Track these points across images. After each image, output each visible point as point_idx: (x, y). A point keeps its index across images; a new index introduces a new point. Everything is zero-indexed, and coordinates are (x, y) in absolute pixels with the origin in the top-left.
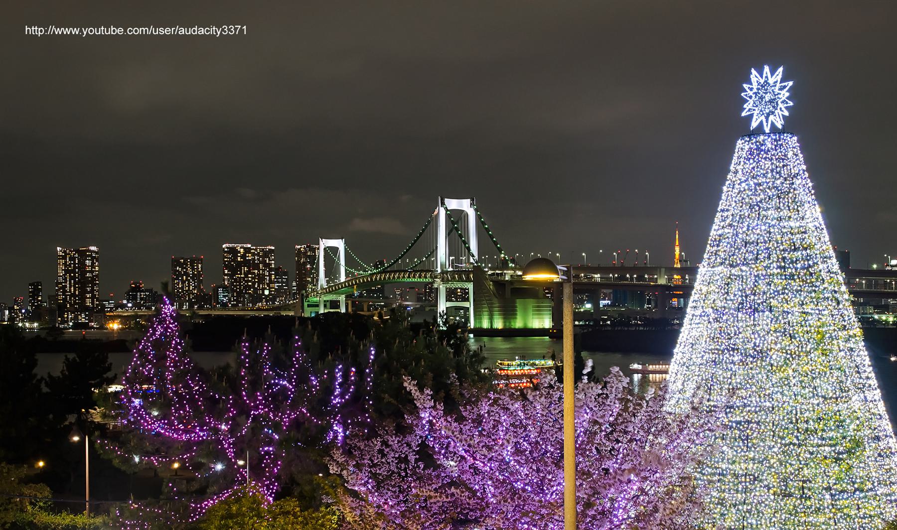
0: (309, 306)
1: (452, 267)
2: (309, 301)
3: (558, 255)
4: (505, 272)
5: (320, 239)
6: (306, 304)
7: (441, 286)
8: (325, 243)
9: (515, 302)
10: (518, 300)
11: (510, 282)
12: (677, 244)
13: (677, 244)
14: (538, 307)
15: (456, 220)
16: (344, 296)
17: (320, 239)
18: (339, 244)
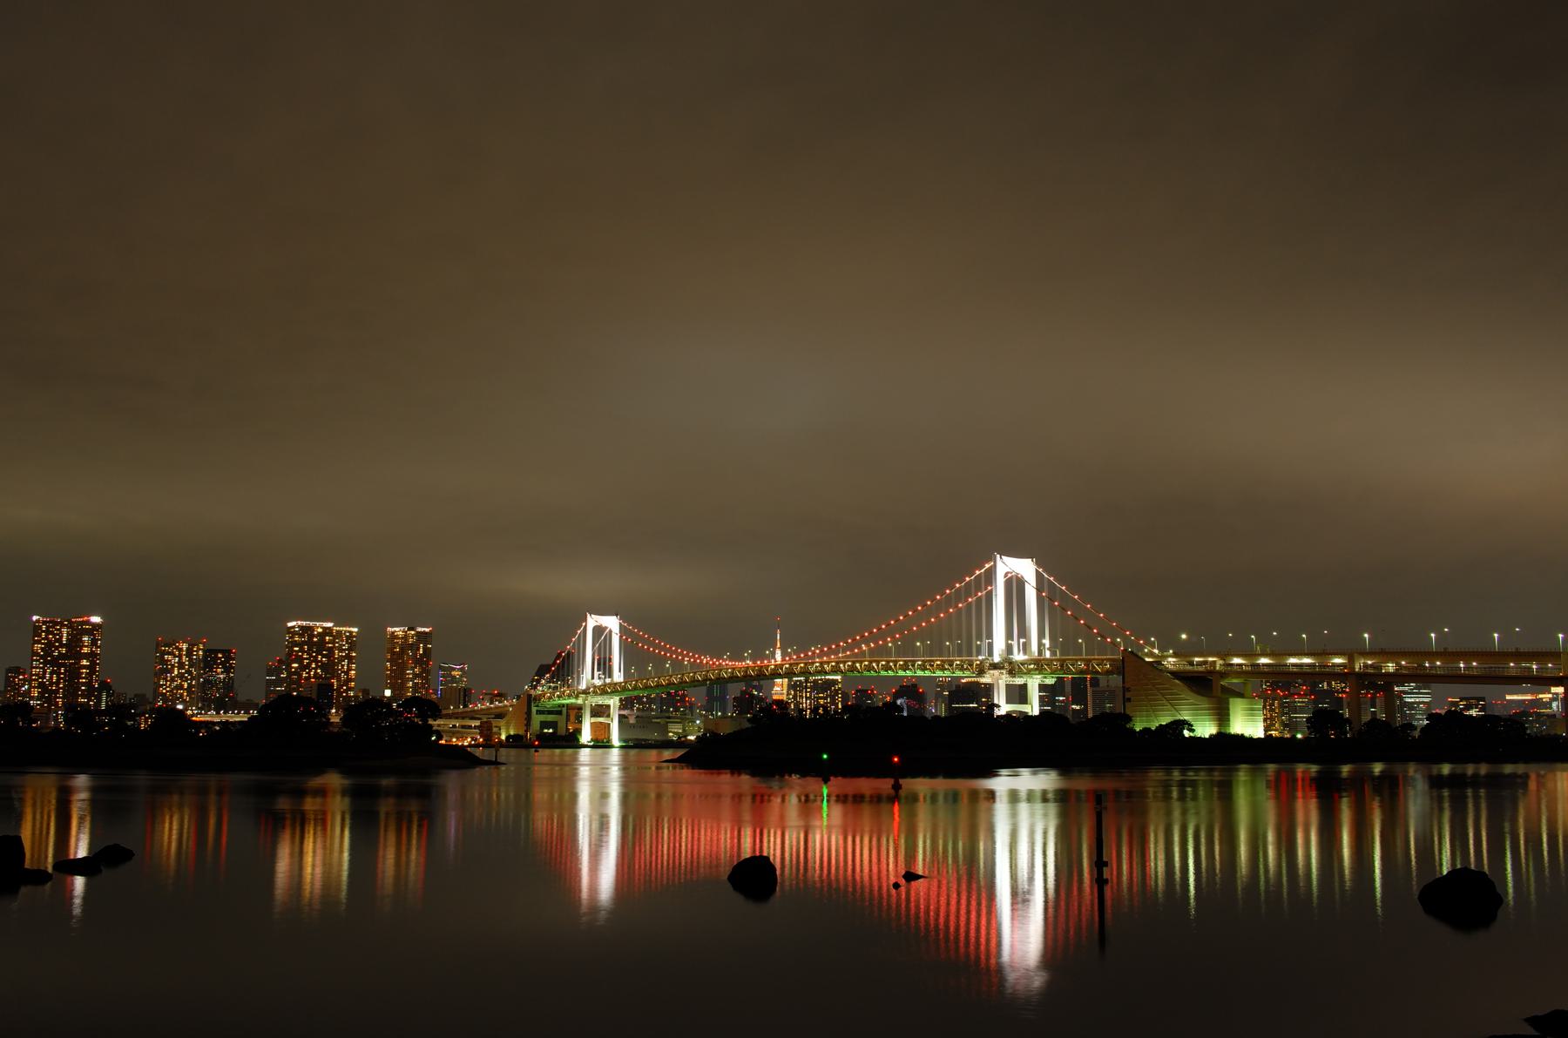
0: (539, 712)
1: (1025, 653)
2: (537, 706)
3: (1304, 636)
5: (588, 615)
6: (534, 709)
8: (592, 621)
9: (1228, 703)
11: (1223, 675)
12: (779, 645)
13: (779, 645)
14: (1252, 709)
15: (1015, 586)
16: (617, 699)
17: (588, 615)
18: (612, 623)
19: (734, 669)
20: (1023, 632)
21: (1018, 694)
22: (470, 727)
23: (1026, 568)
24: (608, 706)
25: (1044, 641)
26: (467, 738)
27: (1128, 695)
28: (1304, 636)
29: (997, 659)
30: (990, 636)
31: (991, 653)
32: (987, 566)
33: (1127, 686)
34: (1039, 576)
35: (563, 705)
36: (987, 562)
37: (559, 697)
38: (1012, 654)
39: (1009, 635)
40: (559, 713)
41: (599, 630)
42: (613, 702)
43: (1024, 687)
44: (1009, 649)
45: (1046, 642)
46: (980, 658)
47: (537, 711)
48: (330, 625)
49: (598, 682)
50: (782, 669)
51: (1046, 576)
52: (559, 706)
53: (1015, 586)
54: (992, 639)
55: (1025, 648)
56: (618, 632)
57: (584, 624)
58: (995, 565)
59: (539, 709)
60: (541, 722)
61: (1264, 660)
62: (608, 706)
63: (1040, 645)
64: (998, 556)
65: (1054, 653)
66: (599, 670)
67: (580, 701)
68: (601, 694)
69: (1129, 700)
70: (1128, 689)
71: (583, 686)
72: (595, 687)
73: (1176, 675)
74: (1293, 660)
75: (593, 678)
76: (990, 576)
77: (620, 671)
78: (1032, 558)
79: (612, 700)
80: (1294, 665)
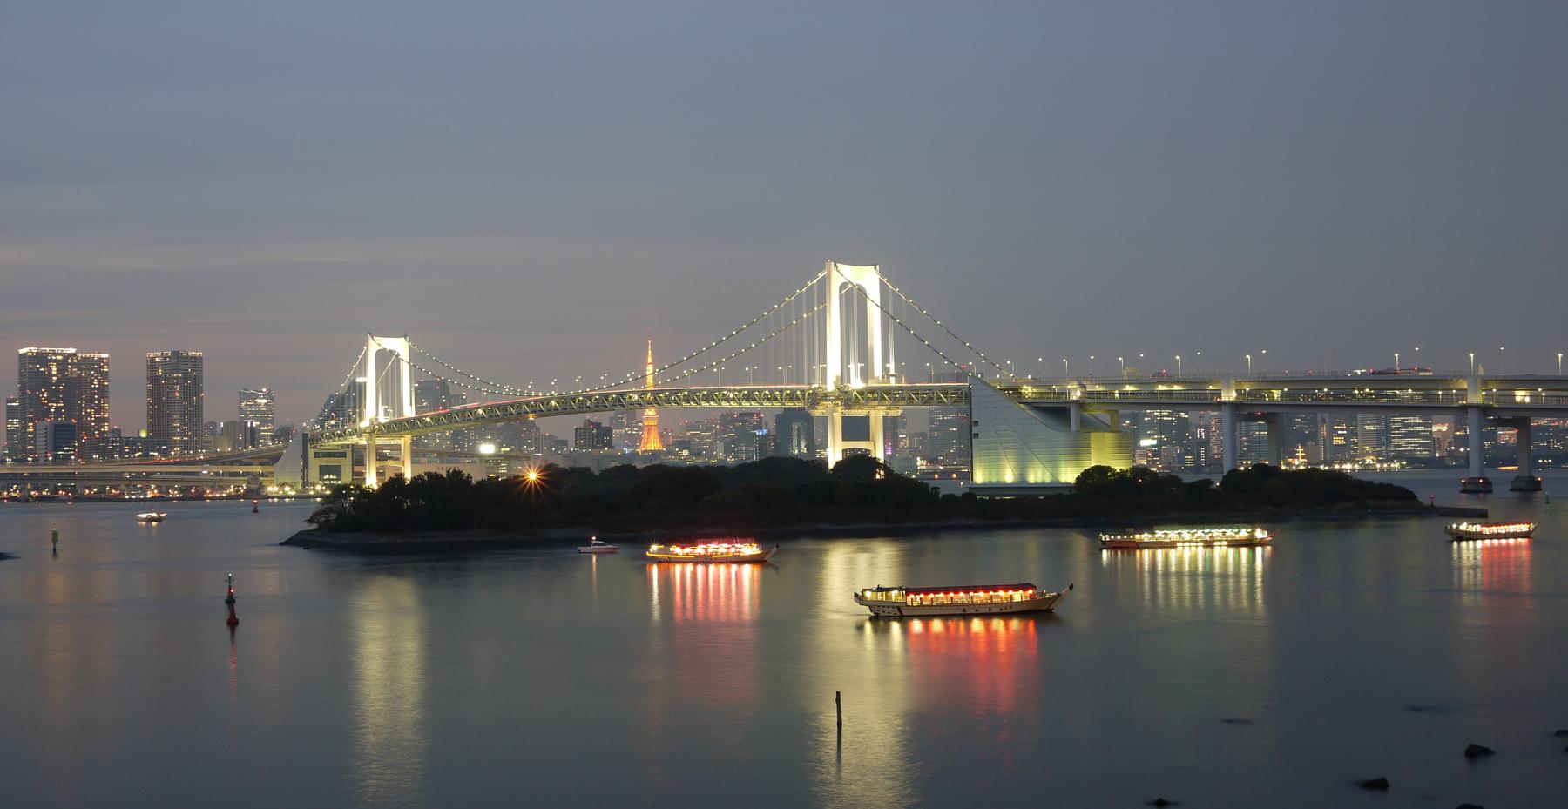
0: (316, 455)
3: (1178, 357)
4: (1069, 387)
6: (311, 452)
7: (834, 414)
8: (375, 345)
9: (1088, 438)
10: (1092, 433)
11: (1080, 405)
12: (650, 360)
13: (650, 360)
15: (854, 298)
16: (409, 437)
18: (400, 346)
19: (535, 401)
20: (865, 355)
21: (858, 428)
22: (237, 474)
23: (868, 278)
24: (400, 445)
25: (888, 365)
26: (229, 487)
27: (975, 430)
28: (1178, 357)
29: (830, 387)
30: (823, 359)
31: (824, 382)
32: (820, 276)
33: (974, 419)
34: (883, 286)
35: (348, 446)
36: (822, 269)
37: (339, 436)
38: (849, 382)
39: (845, 360)
40: (343, 455)
41: (384, 356)
42: (405, 441)
43: (867, 419)
44: (845, 375)
45: (891, 366)
46: (813, 386)
47: (315, 453)
48: (72, 351)
49: (383, 419)
50: (591, 400)
51: (891, 287)
52: (342, 446)
53: (854, 298)
54: (825, 363)
55: (866, 373)
56: (407, 359)
57: (365, 348)
58: (829, 276)
59: (316, 450)
60: (321, 467)
61: (1129, 388)
62: (397, 448)
63: (885, 370)
64: (833, 263)
65: (899, 380)
66: (382, 405)
67: (363, 442)
68: (388, 432)
69: (977, 435)
70: (977, 423)
71: (364, 424)
72: (379, 424)
73: (1034, 405)
74: (1161, 388)
75: (377, 415)
76: (824, 284)
77: (411, 405)
78: (875, 265)
79: (403, 439)
80: (1162, 393)
